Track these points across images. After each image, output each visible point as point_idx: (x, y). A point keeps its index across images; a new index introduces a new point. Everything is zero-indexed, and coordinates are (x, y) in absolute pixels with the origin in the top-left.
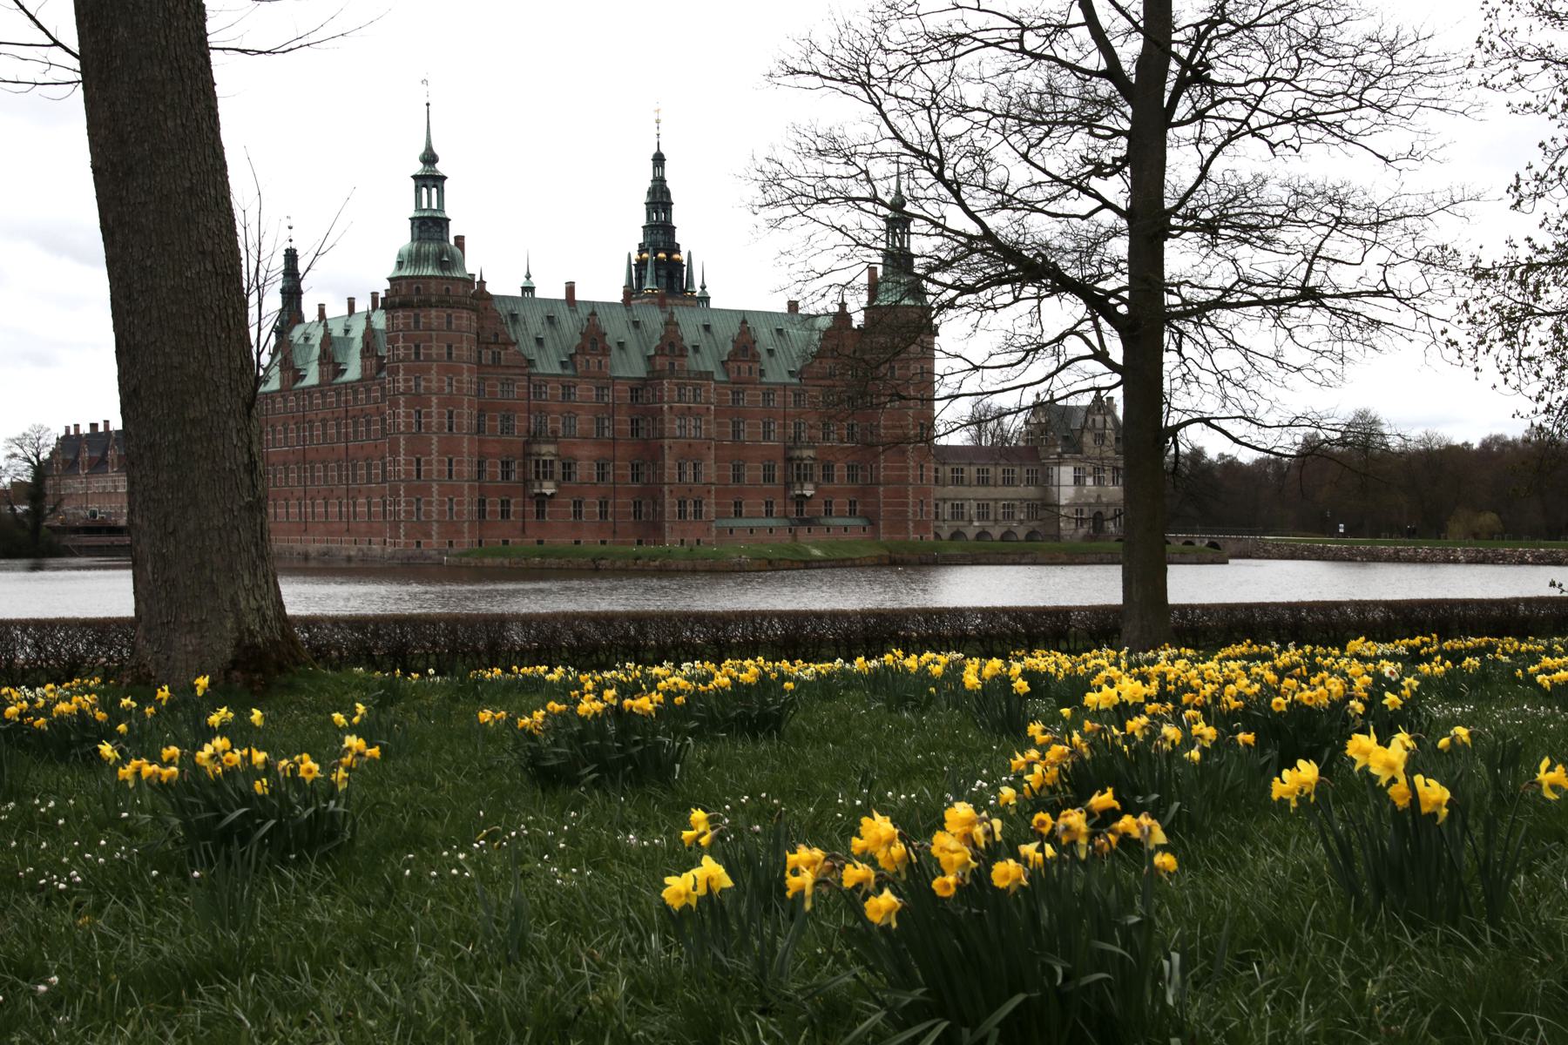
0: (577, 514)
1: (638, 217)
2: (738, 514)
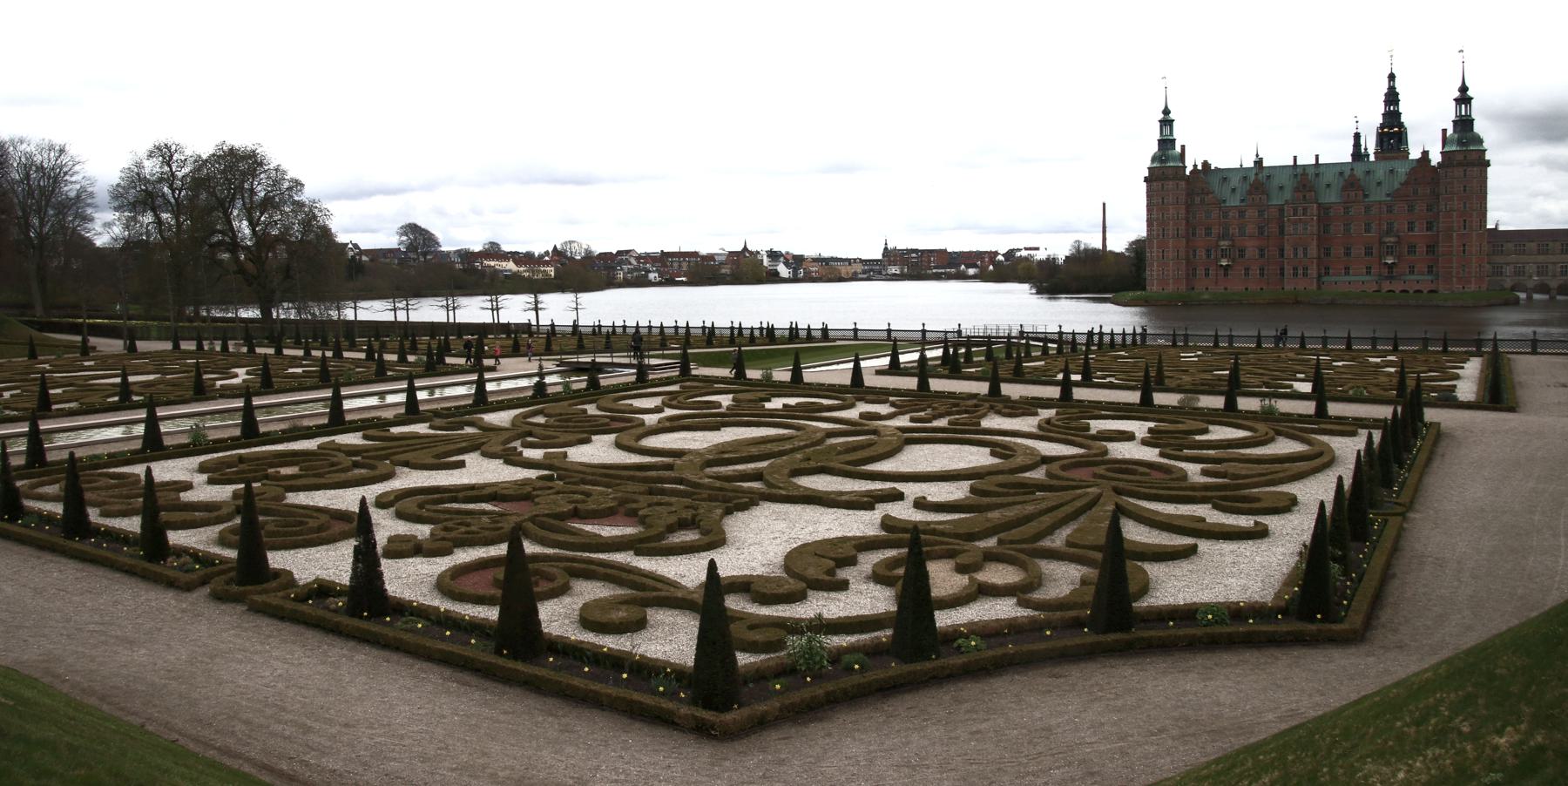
0: (1247, 274)
1: (1381, 108)
2: (1347, 273)
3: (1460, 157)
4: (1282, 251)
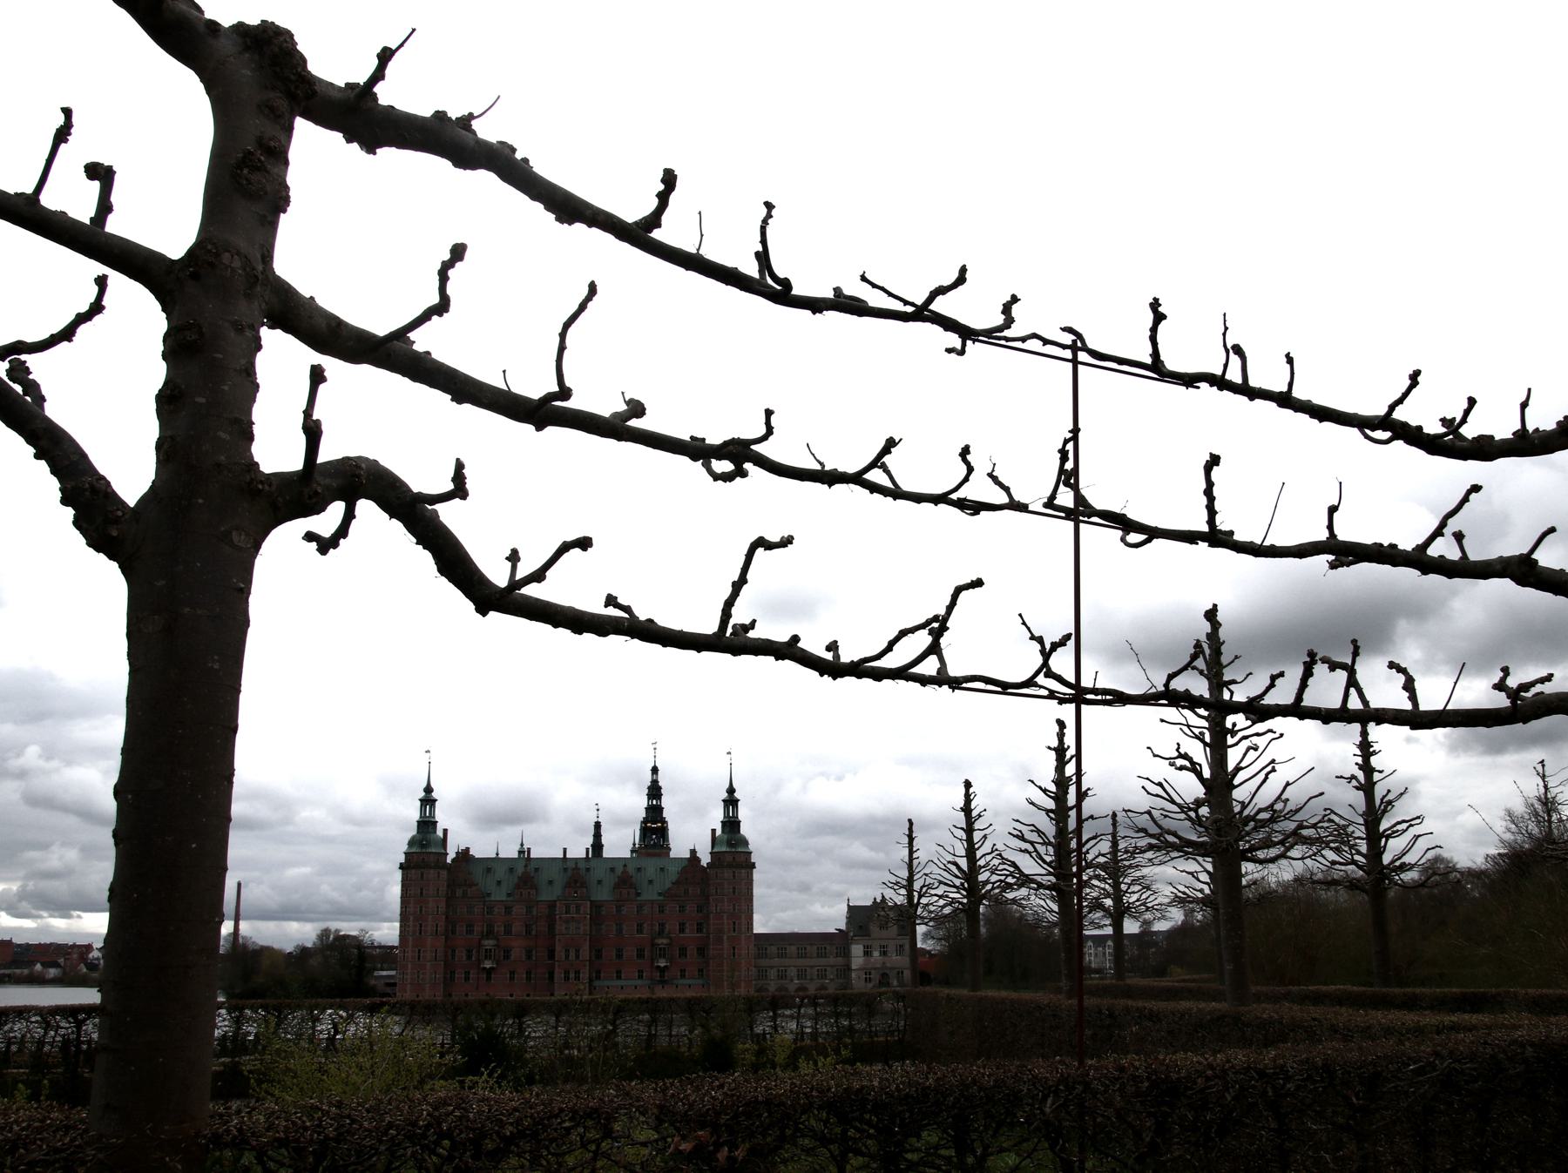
0: (512, 978)
2: (619, 977)
3: (729, 858)
4: (551, 955)
